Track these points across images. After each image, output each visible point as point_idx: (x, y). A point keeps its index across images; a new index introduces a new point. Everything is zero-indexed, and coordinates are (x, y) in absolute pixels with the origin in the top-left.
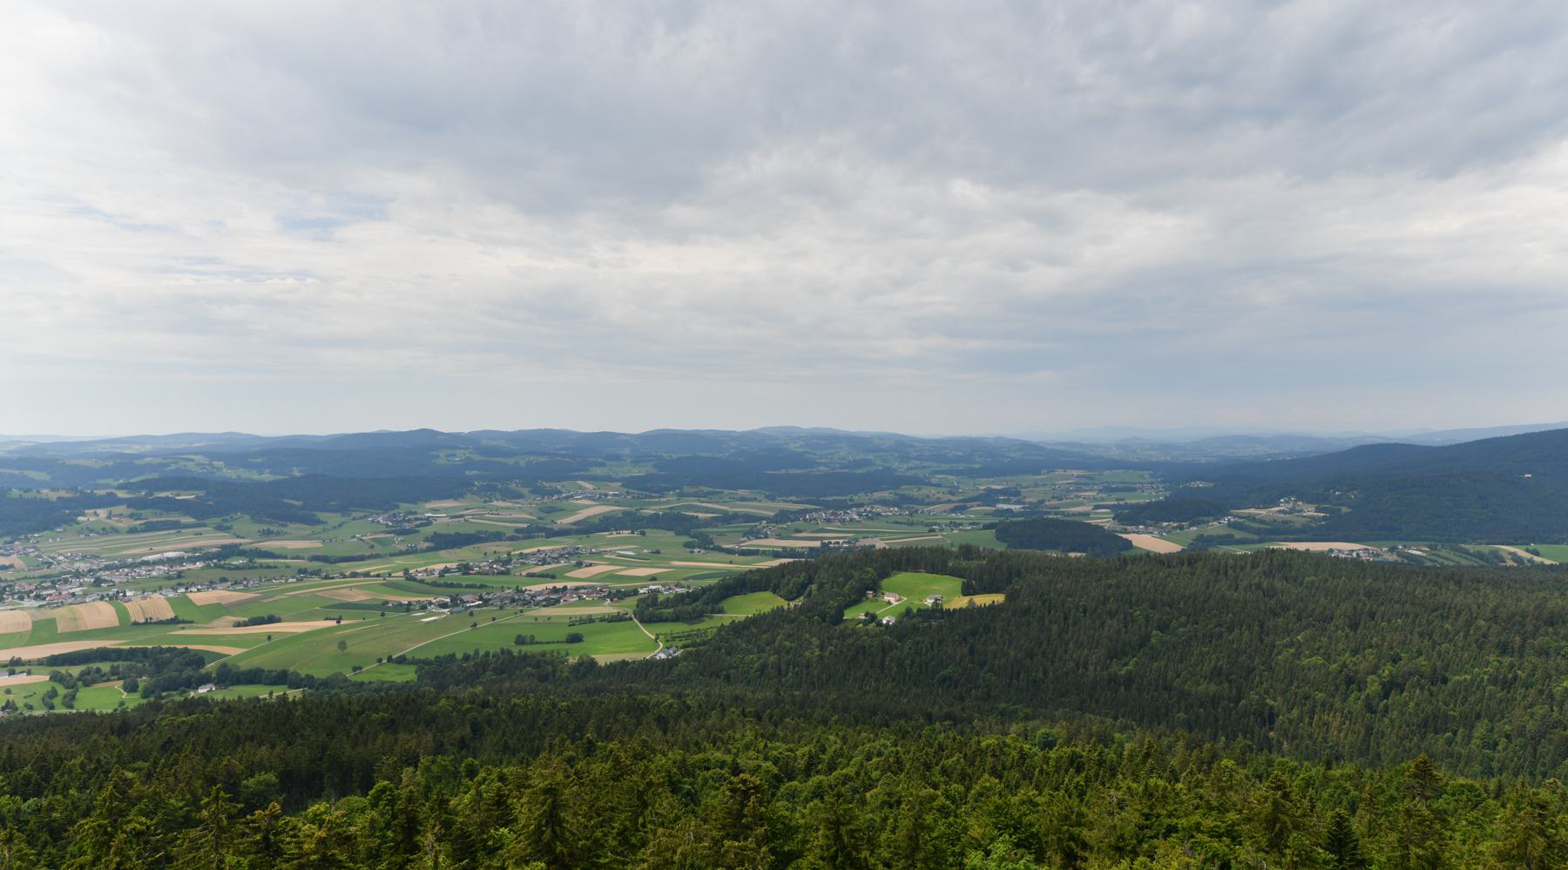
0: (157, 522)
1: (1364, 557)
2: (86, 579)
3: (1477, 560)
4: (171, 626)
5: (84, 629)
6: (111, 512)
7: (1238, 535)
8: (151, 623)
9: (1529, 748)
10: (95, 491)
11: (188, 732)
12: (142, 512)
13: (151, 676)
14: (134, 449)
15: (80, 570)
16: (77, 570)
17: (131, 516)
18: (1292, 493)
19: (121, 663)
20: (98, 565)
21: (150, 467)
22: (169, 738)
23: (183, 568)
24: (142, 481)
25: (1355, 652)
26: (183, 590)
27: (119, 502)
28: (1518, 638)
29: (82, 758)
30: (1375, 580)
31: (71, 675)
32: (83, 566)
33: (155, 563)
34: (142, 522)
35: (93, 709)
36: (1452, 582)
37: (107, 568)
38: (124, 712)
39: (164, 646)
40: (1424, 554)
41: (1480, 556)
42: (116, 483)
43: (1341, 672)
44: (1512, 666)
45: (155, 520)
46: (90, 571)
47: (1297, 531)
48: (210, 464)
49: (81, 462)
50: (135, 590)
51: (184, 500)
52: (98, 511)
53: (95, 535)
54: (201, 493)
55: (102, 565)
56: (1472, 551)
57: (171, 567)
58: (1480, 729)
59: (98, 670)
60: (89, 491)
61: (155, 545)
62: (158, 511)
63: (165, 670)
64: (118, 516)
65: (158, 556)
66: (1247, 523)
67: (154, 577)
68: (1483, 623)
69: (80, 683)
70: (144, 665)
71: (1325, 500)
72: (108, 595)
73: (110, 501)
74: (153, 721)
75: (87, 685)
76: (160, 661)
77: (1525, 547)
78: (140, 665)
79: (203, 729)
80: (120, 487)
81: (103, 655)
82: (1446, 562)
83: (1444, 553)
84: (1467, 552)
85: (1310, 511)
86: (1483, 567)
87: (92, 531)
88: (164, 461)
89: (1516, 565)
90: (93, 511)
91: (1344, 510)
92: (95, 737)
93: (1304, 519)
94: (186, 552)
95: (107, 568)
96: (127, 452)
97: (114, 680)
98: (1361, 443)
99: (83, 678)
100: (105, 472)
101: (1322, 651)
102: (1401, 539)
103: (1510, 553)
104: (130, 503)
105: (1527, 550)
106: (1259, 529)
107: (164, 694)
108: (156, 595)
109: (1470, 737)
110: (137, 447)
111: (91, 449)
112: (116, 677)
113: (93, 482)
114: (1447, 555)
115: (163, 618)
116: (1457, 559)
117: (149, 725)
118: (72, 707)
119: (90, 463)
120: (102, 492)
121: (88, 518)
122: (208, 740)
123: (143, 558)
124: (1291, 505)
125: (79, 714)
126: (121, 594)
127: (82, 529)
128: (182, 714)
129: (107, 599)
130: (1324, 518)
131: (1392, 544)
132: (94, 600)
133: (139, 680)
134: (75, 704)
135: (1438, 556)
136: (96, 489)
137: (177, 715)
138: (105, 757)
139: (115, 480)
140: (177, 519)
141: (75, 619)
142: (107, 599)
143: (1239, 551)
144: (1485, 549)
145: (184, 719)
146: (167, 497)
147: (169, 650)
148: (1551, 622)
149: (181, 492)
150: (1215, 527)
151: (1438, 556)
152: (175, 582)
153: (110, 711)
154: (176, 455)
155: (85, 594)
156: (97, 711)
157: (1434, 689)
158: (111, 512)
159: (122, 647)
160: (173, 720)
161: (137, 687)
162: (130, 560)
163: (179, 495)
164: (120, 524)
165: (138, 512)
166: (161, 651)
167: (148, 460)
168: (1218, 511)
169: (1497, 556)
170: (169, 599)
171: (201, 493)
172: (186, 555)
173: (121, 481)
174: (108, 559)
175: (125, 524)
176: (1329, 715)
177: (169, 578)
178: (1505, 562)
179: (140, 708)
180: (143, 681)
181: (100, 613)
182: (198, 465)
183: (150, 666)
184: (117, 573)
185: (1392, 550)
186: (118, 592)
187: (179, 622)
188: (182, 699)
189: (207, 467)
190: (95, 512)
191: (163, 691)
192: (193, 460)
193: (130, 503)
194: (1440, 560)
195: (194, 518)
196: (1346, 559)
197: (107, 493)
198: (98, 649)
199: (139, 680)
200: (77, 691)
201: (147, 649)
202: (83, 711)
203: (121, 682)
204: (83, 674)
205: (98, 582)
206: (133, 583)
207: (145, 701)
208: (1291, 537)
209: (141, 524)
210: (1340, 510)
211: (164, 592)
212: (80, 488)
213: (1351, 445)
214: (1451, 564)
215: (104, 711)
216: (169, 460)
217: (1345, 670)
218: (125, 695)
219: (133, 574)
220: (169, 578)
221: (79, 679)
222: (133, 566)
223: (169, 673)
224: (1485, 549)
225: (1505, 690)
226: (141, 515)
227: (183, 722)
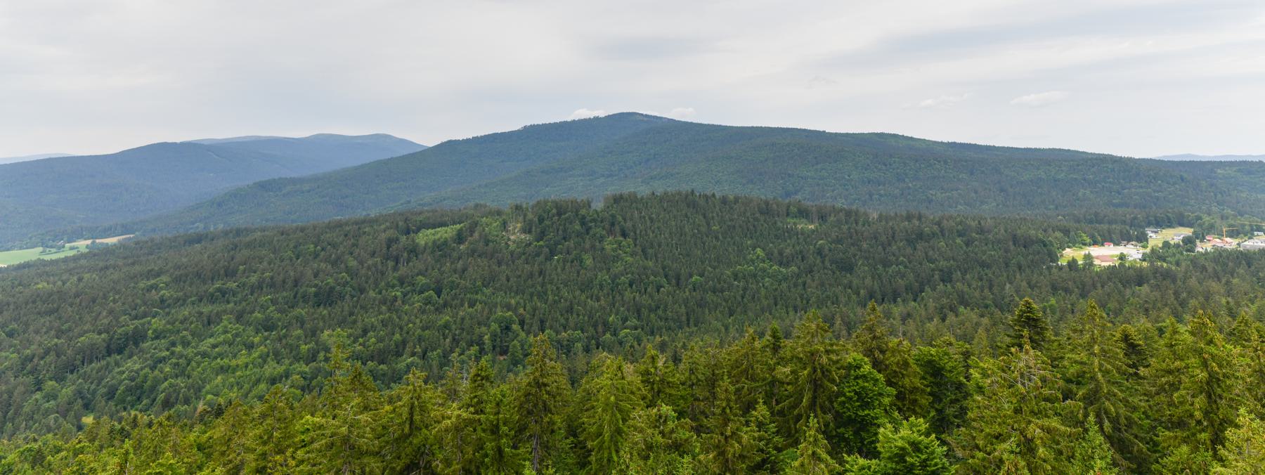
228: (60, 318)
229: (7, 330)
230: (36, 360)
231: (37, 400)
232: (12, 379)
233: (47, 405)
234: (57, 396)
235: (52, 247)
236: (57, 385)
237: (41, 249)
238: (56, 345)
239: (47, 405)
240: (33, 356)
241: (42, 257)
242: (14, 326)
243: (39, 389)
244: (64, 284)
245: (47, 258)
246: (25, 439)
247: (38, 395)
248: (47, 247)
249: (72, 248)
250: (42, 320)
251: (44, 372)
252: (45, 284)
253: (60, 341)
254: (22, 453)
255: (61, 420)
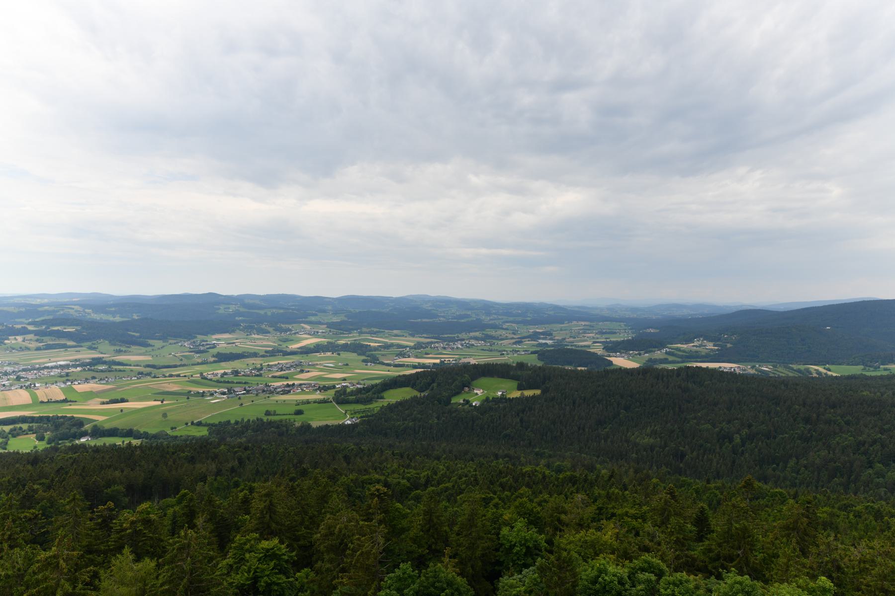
0: (53, 344)
1: (738, 371)
2: (11, 377)
3: (796, 373)
4: (63, 404)
5: (11, 405)
6: (24, 338)
7: (671, 358)
8: (51, 402)
9: (816, 473)
10: (14, 326)
11: (73, 463)
12: (43, 338)
13: (52, 432)
14: (38, 301)
15: (8, 371)
16: (6, 371)
17: (37, 341)
18: (701, 336)
19: (34, 424)
20: (18, 368)
21: (48, 312)
22: (61, 466)
23: (69, 371)
24: (43, 320)
25: (729, 422)
26: (70, 383)
27: (30, 332)
28: (815, 415)
29: (9, 477)
30: (742, 384)
31: (4, 431)
32: (9, 369)
33: (52, 368)
34: (44, 344)
35: (18, 450)
36: (783, 385)
37: (24, 370)
38: (37, 452)
39: (59, 415)
40: (770, 370)
41: (799, 371)
42: (27, 321)
43: (720, 432)
44: (810, 430)
45: (51, 343)
46: (14, 372)
47: (703, 357)
48: (84, 311)
49: (5, 309)
50: (41, 383)
51: (68, 331)
52: (17, 337)
53: (16, 351)
54: (79, 328)
55: (21, 368)
56: (795, 369)
57: (62, 370)
58: (792, 463)
59: (21, 428)
60: (11, 326)
61: (53, 357)
62: (54, 338)
63: (60, 429)
64: (28, 340)
65: (55, 363)
66: (676, 352)
67: (52, 376)
68: (797, 407)
69: (10, 436)
70: (48, 426)
71: (719, 340)
72: (25, 386)
73: (24, 332)
74: (53, 457)
75: (14, 436)
76: (57, 423)
77: (823, 366)
78: (46, 425)
79: (81, 461)
80: (29, 324)
81: (24, 420)
82: (781, 374)
83: (780, 369)
84: (792, 369)
85: (710, 346)
86: (800, 377)
87: (14, 349)
88: (56, 309)
89: (817, 376)
90: (13, 337)
91: (729, 345)
92: (17, 466)
93: (707, 350)
94: (71, 362)
95: (24, 370)
96: (33, 303)
97: (30, 434)
98: (740, 309)
99: (12, 433)
100: (21, 315)
101: (711, 421)
102: (758, 362)
103: (815, 370)
104: (36, 333)
105: (824, 368)
106: (683, 355)
107: (60, 442)
108: (54, 386)
109: (786, 467)
110: (39, 300)
111: (12, 301)
112: (31, 432)
113: (12, 320)
114: (782, 371)
115: (58, 399)
116: (786, 372)
117: (50, 459)
118: (6, 449)
119: (11, 309)
120: (19, 326)
121: (11, 341)
122: (84, 468)
123: (45, 365)
124: (700, 343)
125: (9, 453)
126: (33, 385)
127: (8, 348)
128: (70, 453)
129: (24, 388)
130: (718, 350)
131: (753, 364)
132: (16, 389)
133: (45, 434)
134: (7, 447)
135: (778, 371)
136: (15, 325)
137: (67, 453)
138: (23, 477)
139: (27, 320)
140: (65, 342)
141: (5, 399)
142: (24, 388)
143: (670, 367)
144: (802, 367)
145: (71, 456)
146: (58, 330)
147: (62, 417)
148: (834, 406)
149: (66, 327)
150: (658, 354)
151: (778, 371)
152: (64, 379)
153: (27, 451)
154: (62, 306)
155: (11, 385)
156: (20, 451)
157: (768, 441)
158: (24, 338)
159: (34, 415)
160: (65, 456)
161: (44, 438)
162: (37, 366)
163: (65, 329)
164: (30, 345)
165: (41, 338)
166: (58, 418)
167: (46, 308)
168: (660, 345)
169: (808, 371)
170: (61, 389)
171: (79, 328)
172: (71, 363)
173: (30, 320)
174: (24, 365)
175: (34, 345)
176: (712, 455)
177: (61, 376)
178: (812, 374)
179: (46, 450)
180: (47, 435)
181: (21, 396)
182: (76, 311)
183: (52, 426)
184: (30, 373)
185: (753, 367)
186: (31, 384)
187: (68, 402)
188: (70, 445)
189: (82, 312)
190: (15, 338)
191: (60, 440)
192: (73, 309)
193: (36, 333)
194: (778, 373)
195: (75, 342)
196: (727, 372)
197: (22, 327)
198: (20, 416)
199: (45, 434)
200: (9, 440)
201: (49, 416)
202: (12, 451)
203: (35, 435)
204: (11, 430)
205: (18, 378)
206: (39, 379)
207: (49, 446)
208: (699, 360)
209: (43, 345)
210: (726, 345)
211: (58, 384)
212: (5, 324)
213: (735, 310)
214: (784, 375)
215: (24, 451)
216: (58, 309)
217: (723, 431)
218: (37, 443)
219: (40, 374)
220: (61, 376)
221: (9, 433)
222: (39, 369)
223: (63, 430)
224: (802, 367)
225: (806, 443)
226: (43, 340)
227: (70, 458)
228: (882, 420)
229: (845, 419)
230: (867, 446)
231: (869, 473)
232: (852, 454)
233: (878, 480)
234: (885, 476)
235: (870, 366)
236: (884, 468)
237: (862, 367)
238: (880, 438)
239: (878, 480)
240: (865, 442)
241: (864, 373)
242: (849, 418)
243: (871, 467)
244: (882, 396)
245: (868, 374)
246: (865, 498)
247: (870, 471)
248: (867, 366)
249: (885, 370)
250: (869, 419)
251: (873, 456)
252: (868, 393)
253: (883, 437)
254: (867, 507)
255: (889, 494)
